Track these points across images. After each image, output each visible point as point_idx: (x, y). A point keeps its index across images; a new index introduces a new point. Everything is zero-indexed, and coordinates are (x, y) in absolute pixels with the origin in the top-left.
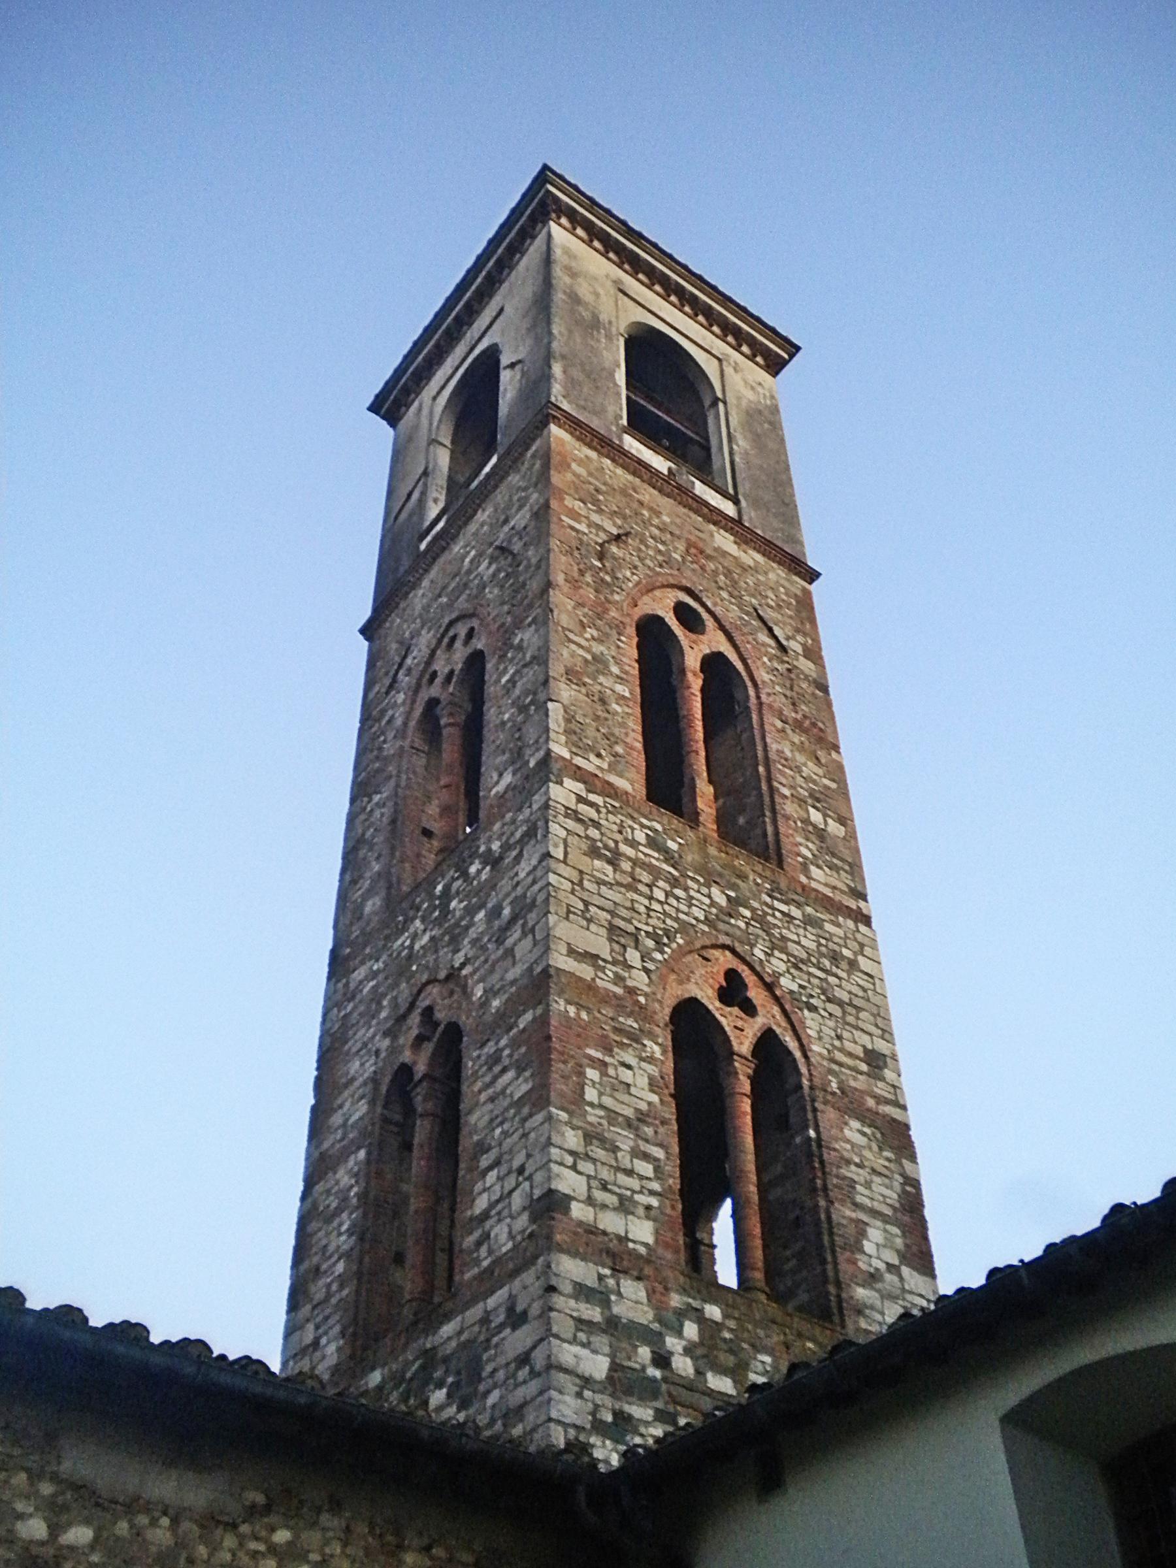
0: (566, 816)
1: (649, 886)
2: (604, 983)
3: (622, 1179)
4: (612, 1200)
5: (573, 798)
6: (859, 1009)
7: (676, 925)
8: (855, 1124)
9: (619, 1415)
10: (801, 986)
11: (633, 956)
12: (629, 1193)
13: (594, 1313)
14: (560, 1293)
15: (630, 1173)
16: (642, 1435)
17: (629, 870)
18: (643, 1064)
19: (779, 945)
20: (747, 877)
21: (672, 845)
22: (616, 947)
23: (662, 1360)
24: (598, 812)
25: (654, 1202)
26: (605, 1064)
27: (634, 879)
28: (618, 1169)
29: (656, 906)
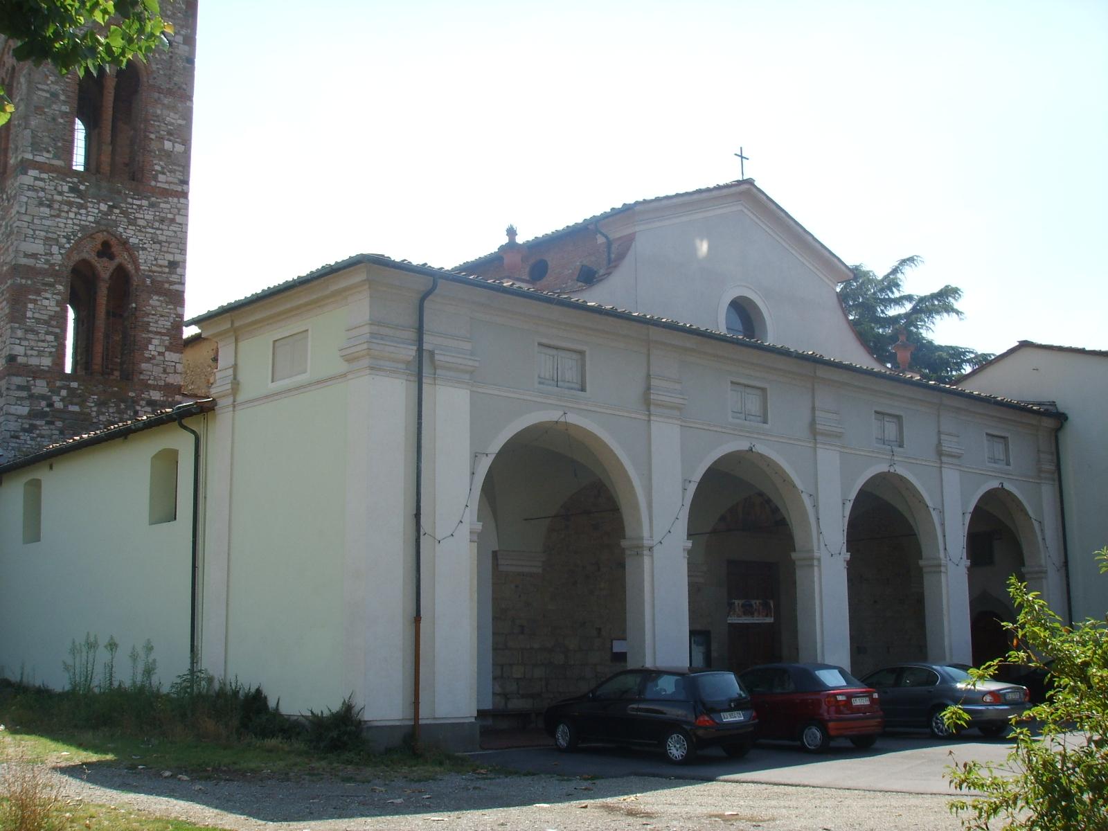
0: (29, 190)
1: (67, 212)
2: (40, 264)
3: (41, 344)
4: (35, 353)
5: (32, 179)
6: (170, 243)
7: (78, 228)
8: (155, 297)
9: (31, 425)
10: (140, 240)
11: (55, 249)
12: (42, 349)
13: (24, 394)
14: (11, 390)
15: (43, 341)
16: (40, 430)
17: (58, 207)
18: (54, 296)
19: (132, 222)
20: (121, 192)
21: (82, 187)
22: (47, 247)
23: (51, 405)
24: (45, 182)
25: (54, 350)
26: (37, 300)
27: (60, 211)
28: (39, 341)
29: (70, 222)
